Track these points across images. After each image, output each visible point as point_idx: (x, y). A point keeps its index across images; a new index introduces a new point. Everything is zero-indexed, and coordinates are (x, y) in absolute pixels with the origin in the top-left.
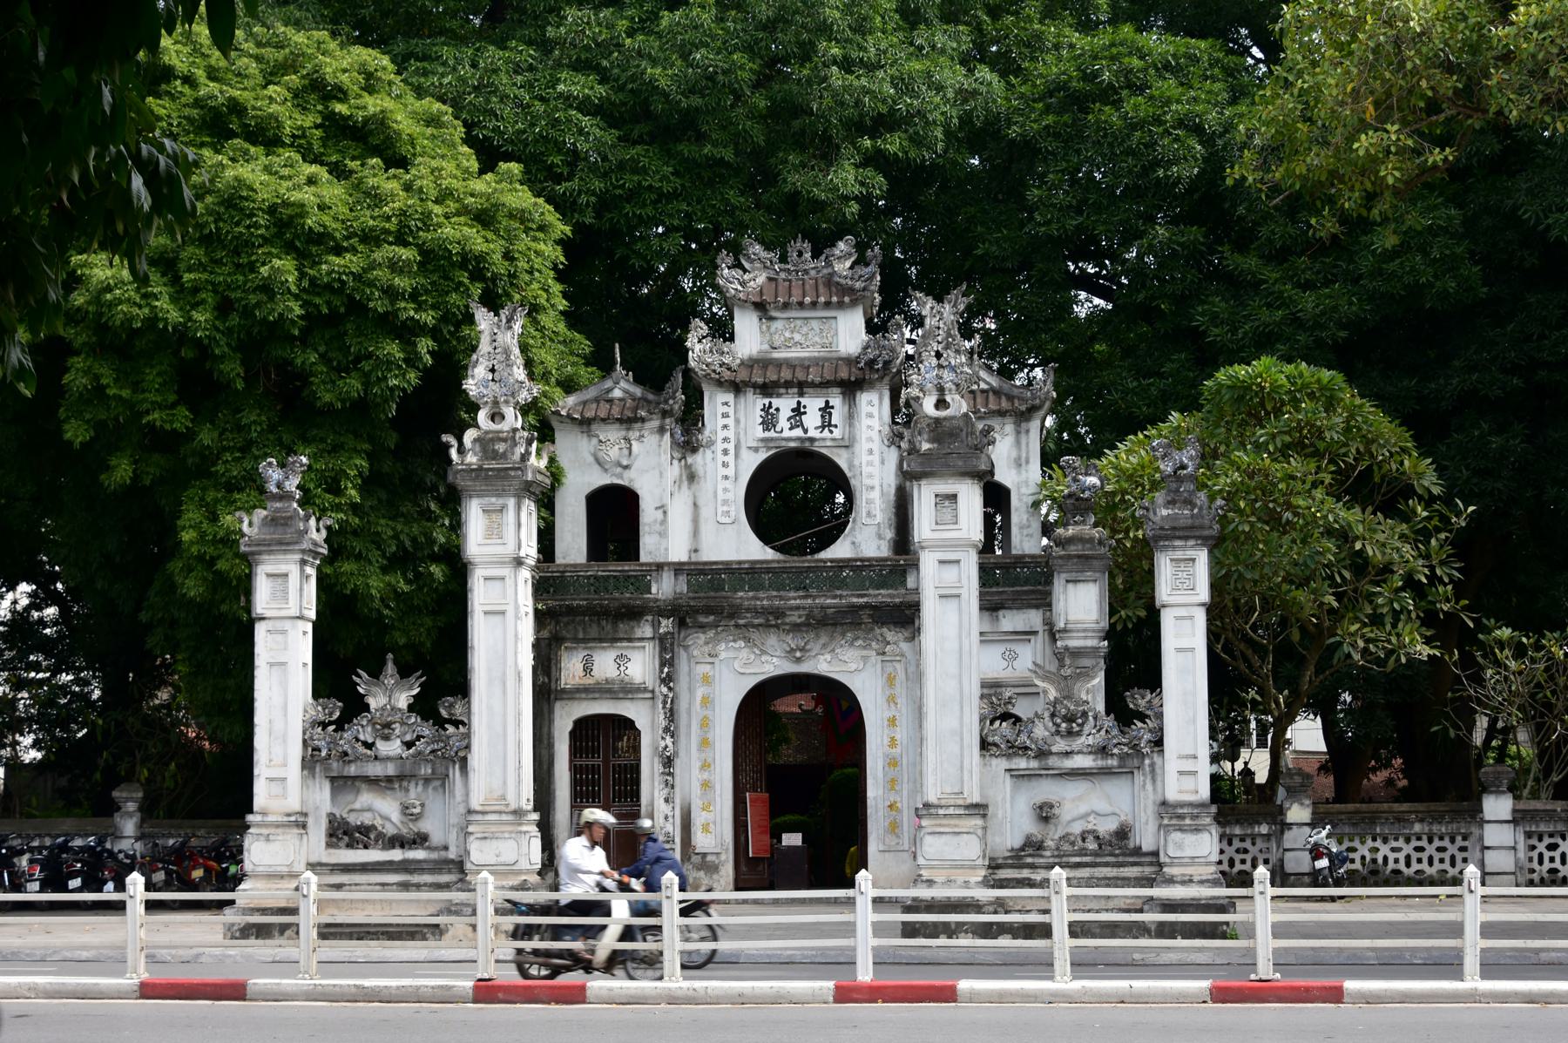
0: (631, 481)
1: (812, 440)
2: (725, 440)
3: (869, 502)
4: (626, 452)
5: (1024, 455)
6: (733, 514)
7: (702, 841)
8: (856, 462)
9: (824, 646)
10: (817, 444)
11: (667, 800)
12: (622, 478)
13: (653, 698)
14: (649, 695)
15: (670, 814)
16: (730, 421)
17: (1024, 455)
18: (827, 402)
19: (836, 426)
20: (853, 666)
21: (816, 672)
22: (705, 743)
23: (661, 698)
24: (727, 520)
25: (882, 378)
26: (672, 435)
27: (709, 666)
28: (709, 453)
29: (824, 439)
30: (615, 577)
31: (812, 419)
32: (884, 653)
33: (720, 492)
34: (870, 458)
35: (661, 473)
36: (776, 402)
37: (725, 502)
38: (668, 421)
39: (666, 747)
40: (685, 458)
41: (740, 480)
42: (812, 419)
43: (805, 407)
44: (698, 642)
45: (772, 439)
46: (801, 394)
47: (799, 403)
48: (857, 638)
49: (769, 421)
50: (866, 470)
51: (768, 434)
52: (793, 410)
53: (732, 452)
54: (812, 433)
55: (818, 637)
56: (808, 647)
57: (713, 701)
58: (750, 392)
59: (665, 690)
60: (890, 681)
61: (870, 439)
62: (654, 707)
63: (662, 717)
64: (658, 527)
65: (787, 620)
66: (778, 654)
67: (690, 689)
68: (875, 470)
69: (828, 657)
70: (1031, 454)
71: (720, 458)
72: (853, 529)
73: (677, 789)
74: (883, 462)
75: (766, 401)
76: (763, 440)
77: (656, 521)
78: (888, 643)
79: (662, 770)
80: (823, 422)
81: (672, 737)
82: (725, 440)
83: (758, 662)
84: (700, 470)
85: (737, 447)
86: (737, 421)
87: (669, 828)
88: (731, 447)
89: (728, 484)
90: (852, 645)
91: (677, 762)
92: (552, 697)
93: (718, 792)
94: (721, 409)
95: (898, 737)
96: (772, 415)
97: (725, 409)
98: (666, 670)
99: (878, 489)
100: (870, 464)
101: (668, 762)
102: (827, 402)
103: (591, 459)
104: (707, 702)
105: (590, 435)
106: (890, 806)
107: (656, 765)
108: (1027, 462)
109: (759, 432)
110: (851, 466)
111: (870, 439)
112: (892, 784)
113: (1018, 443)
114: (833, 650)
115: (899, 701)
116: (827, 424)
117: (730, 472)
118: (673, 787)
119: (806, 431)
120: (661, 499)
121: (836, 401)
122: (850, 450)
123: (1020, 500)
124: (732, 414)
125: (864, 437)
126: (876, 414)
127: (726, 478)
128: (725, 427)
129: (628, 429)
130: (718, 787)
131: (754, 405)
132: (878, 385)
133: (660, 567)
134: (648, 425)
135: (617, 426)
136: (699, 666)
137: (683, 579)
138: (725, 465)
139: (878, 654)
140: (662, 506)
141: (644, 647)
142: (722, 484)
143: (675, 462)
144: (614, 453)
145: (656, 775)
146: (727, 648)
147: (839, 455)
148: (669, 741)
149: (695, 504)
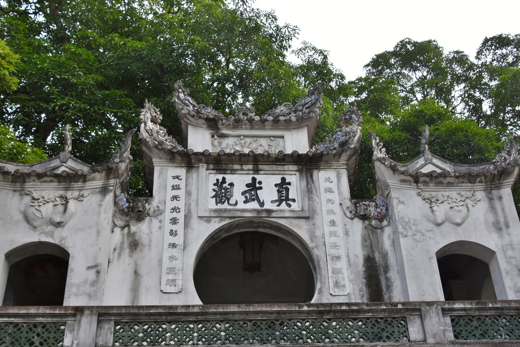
0: (62, 239)
2: (175, 209)
3: (336, 272)
4: (61, 208)
5: (502, 220)
6: (179, 283)
8: (318, 233)
10: (274, 214)
12: (52, 236)
16: (181, 193)
17: (502, 220)
18: (283, 179)
19: (294, 200)
24: (172, 289)
25: (338, 155)
26: (116, 203)
28: (155, 222)
29: (281, 211)
30: (16, 325)
33: (166, 259)
34: (333, 229)
35: (98, 232)
36: (229, 178)
37: (171, 270)
38: (112, 181)
40: (128, 226)
43: (260, 183)
45: (226, 210)
46: (256, 171)
47: (254, 179)
50: (329, 240)
51: (220, 206)
52: (248, 185)
53: (181, 221)
54: (268, 206)
58: (203, 168)
61: (331, 212)
68: (340, 240)
71: (168, 226)
74: (347, 233)
75: (220, 177)
76: (215, 211)
77: (86, 281)
80: (280, 197)
84: (145, 239)
85: (187, 217)
86: (188, 193)
88: (181, 217)
89: (174, 252)
94: (172, 182)
96: (226, 189)
97: (176, 182)
99: (344, 259)
100: (333, 234)
102: (283, 179)
103: (20, 217)
105: (23, 193)
108: (507, 226)
109: (212, 204)
110: (313, 237)
111: (331, 212)
113: (493, 208)
117: (179, 240)
119: (262, 204)
120: (95, 258)
122: (311, 222)
123: (509, 263)
125: (324, 209)
126: (335, 189)
127: (174, 246)
128: (175, 198)
129: (67, 189)
132: (335, 164)
133: (79, 310)
134: (89, 184)
135: (55, 184)
137: (108, 327)
138: (173, 233)
140: (96, 266)
142: (168, 252)
143: (117, 230)
144: (47, 210)
147: (299, 227)
149: (136, 273)
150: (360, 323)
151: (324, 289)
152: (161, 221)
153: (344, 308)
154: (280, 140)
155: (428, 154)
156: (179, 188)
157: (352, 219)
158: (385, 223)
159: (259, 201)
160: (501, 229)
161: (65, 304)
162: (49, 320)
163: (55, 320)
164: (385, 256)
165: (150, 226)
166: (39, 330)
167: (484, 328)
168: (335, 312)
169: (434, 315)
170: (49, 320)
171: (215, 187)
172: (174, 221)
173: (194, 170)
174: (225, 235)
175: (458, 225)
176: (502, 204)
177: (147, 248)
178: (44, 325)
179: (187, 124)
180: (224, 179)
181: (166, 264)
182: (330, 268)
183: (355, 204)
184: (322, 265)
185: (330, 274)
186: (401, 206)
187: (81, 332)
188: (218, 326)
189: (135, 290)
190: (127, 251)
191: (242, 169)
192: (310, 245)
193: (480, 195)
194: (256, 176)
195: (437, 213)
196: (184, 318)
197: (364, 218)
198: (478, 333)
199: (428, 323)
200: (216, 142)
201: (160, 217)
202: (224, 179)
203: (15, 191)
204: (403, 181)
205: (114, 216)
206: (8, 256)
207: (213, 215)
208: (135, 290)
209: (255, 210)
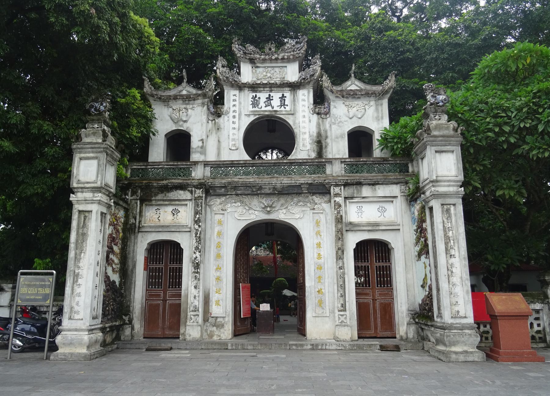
1: (276, 111)
2: (234, 111)
3: (304, 139)
5: (380, 115)
7: (216, 310)
8: (297, 122)
9: (282, 205)
10: (278, 113)
11: (195, 287)
13: (190, 231)
14: (189, 230)
15: (197, 295)
16: (237, 103)
18: (283, 95)
19: (287, 105)
20: (297, 216)
21: (278, 219)
22: (218, 256)
23: (195, 231)
24: (234, 148)
25: (309, 82)
26: (208, 109)
27: (221, 216)
28: (226, 118)
29: (281, 111)
30: (173, 168)
31: (276, 102)
32: (314, 209)
34: (304, 119)
35: (202, 125)
36: (259, 95)
37: (233, 140)
39: (196, 257)
41: (240, 130)
42: (276, 102)
43: (272, 97)
44: (216, 202)
45: (257, 111)
46: (271, 91)
47: (270, 95)
48: (300, 201)
49: (255, 102)
50: (302, 125)
51: (254, 109)
52: (267, 98)
53: (237, 117)
55: (279, 200)
56: (274, 205)
57: (223, 232)
59: (197, 227)
60: (318, 223)
61: (304, 111)
62: (191, 236)
63: (195, 241)
64: (199, 150)
65: (263, 192)
66: (258, 209)
67: (211, 228)
68: (306, 125)
69: (284, 211)
70: (384, 115)
71: (232, 119)
72: (296, 152)
73: (201, 281)
74: (310, 121)
75: (254, 94)
76: (252, 111)
77: (198, 147)
78: (316, 204)
79: (193, 270)
81: (200, 252)
82: (234, 111)
83: (247, 213)
84: (222, 126)
85: (240, 115)
86: (240, 103)
87: (196, 303)
88: (237, 115)
89: (235, 131)
90: (297, 205)
91: (202, 266)
92: (137, 230)
93: (225, 283)
94: (233, 98)
95: (322, 253)
96: (257, 100)
98: (198, 216)
100: (304, 122)
101: (197, 266)
102: (283, 95)
103: (169, 118)
104: (220, 234)
105: (168, 106)
106: (318, 291)
107: (190, 268)
109: (251, 108)
110: (294, 123)
111: (304, 111)
112: (319, 279)
113: (377, 110)
114: (287, 208)
115: (322, 234)
116: (283, 104)
117: (236, 126)
118: (199, 279)
119: (273, 108)
120: (202, 136)
121: (288, 94)
122: (294, 116)
124: (237, 100)
126: (306, 100)
127: (234, 128)
128: (234, 105)
130: (224, 280)
131: (248, 95)
132: (307, 86)
134: (197, 102)
136: (216, 215)
137: (208, 169)
138: (233, 123)
139: (311, 209)
141: (186, 205)
142: (232, 132)
143: (210, 122)
145: (190, 273)
146: (231, 206)
147: (289, 118)
148: (198, 254)
149: (219, 141)
150: (307, 167)
151: (298, 147)
152: (228, 117)
153: (300, 161)
154: (285, 68)
155: (353, 78)
156: (236, 101)
157: (313, 114)
158: (328, 116)
159: (271, 106)
160: (379, 120)
161: (191, 160)
162: (186, 166)
163: (188, 166)
164: (326, 131)
165: (224, 120)
166: (182, 170)
167: (358, 169)
168: (297, 163)
169: (337, 164)
170: (186, 166)
171: (252, 100)
172: (234, 117)
173: (242, 91)
174: (256, 122)
175: (360, 118)
176: (382, 107)
177: (223, 130)
178: (184, 169)
179: (240, 61)
180: (256, 95)
181: (231, 137)
182: (301, 138)
183: (315, 106)
184: (298, 136)
185: (301, 141)
186: (335, 109)
187: (198, 171)
188: (250, 168)
189: (219, 154)
190: (215, 131)
191: (264, 90)
192: (293, 127)
193: (372, 103)
194: (270, 94)
195: (350, 113)
196: (237, 165)
197: (318, 114)
198: (355, 171)
199: (334, 167)
200: (254, 71)
201: (228, 115)
202: (256, 95)
203: (165, 106)
204: (337, 97)
205: (208, 115)
206: (166, 135)
207: (251, 114)
208: (219, 154)
209: (270, 111)
